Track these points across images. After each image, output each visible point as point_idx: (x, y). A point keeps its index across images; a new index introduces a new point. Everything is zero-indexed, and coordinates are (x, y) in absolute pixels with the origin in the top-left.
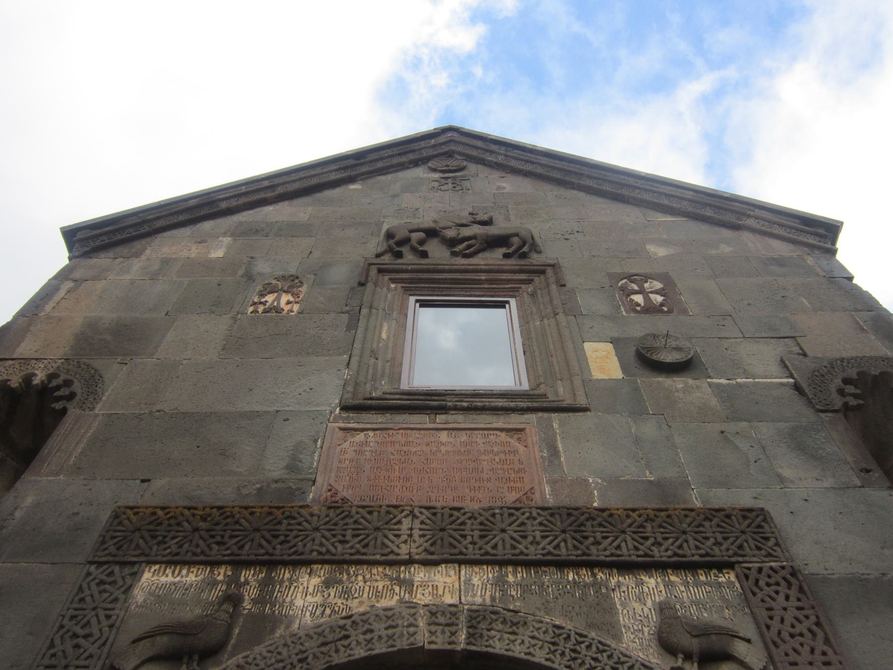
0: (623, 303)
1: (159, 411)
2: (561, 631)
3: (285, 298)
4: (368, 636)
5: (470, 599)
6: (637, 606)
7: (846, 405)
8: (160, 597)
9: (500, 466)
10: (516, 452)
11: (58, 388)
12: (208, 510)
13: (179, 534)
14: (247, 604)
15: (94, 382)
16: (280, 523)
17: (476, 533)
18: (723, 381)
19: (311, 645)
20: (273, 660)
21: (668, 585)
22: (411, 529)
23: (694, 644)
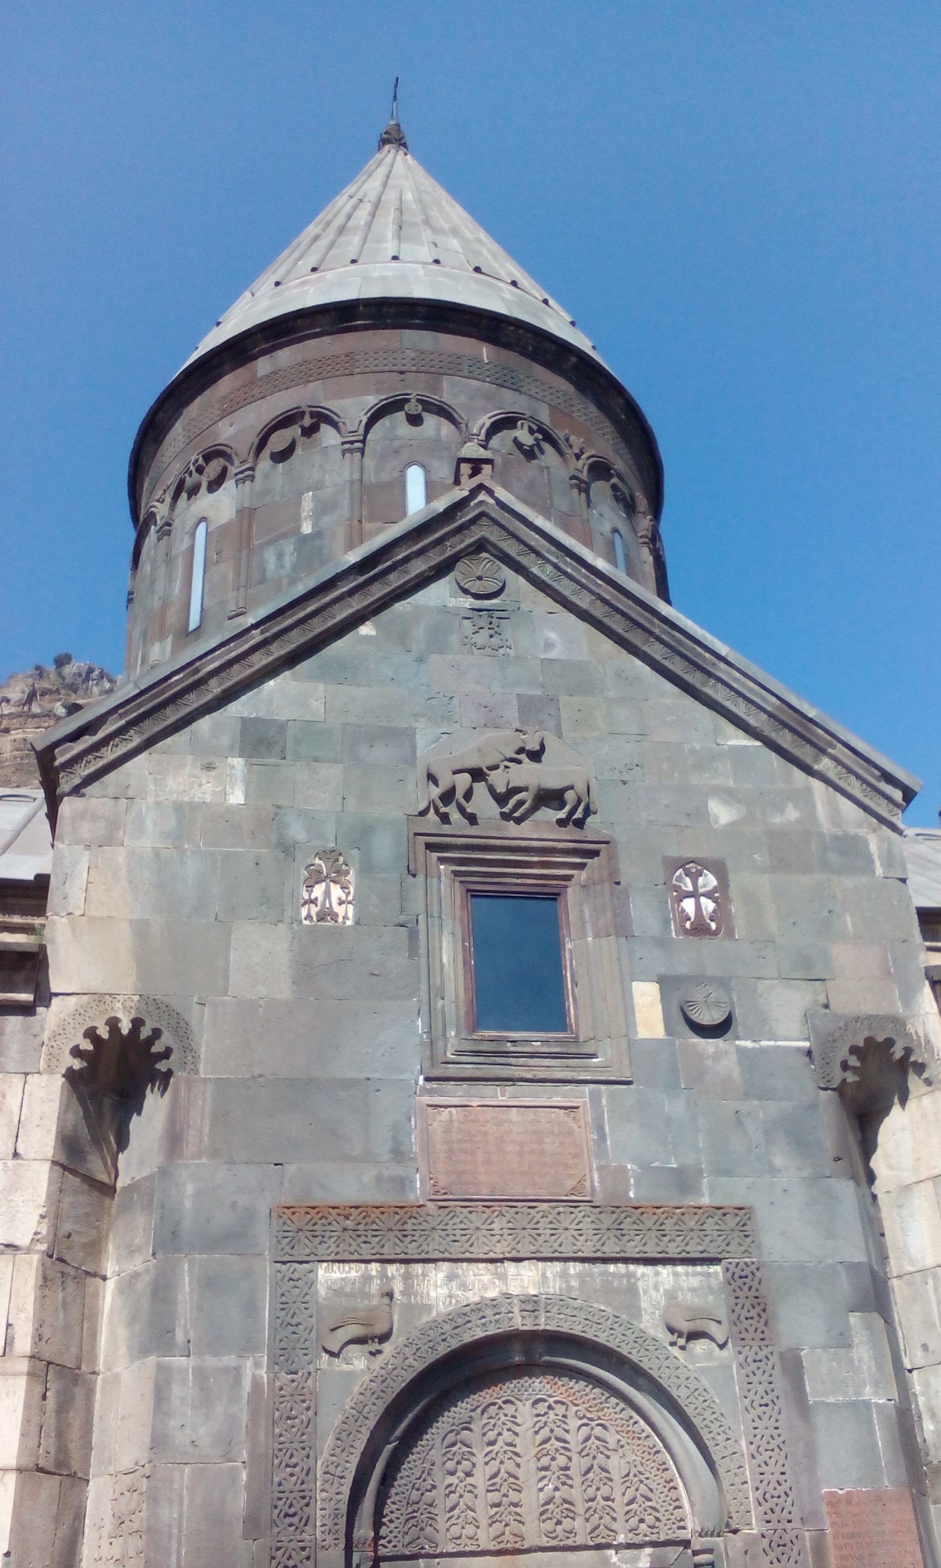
0: (674, 915)
1: (261, 1076)
2: (603, 1313)
3: (336, 892)
4: (483, 1321)
5: (546, 1290)
6: (653, 1293)
7: (844, 1080)
8: (337, 1292)
9: (559, 1150)
10: (570, 1133)
11: (151, 1041)
12: (348, 1209)
13: (333, 1234)
14: (397, 1295)
15: (182, 1028)
16: (406, 1223)
17: (549, 1232)
18: (748, 1044)
19: (447, 1327)
20: (426, 1341)
21: (676, 1274)
22: (501, 1229)
23: (685, 1327)
